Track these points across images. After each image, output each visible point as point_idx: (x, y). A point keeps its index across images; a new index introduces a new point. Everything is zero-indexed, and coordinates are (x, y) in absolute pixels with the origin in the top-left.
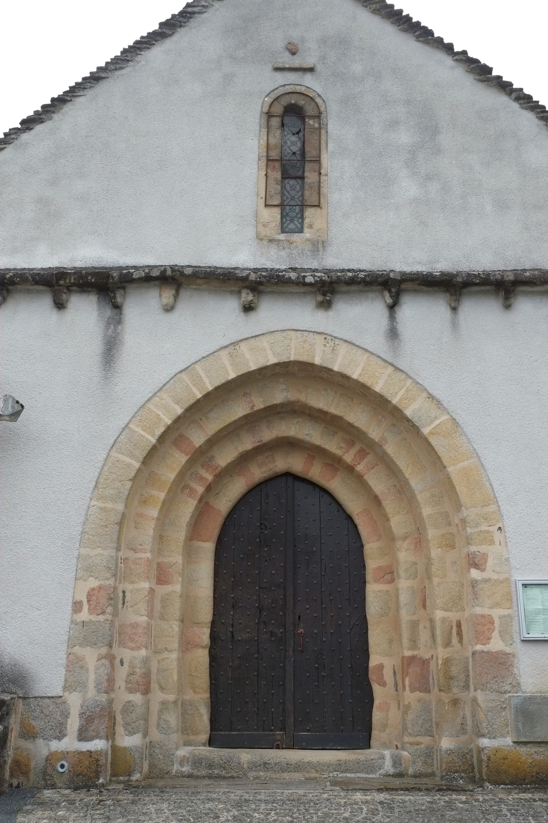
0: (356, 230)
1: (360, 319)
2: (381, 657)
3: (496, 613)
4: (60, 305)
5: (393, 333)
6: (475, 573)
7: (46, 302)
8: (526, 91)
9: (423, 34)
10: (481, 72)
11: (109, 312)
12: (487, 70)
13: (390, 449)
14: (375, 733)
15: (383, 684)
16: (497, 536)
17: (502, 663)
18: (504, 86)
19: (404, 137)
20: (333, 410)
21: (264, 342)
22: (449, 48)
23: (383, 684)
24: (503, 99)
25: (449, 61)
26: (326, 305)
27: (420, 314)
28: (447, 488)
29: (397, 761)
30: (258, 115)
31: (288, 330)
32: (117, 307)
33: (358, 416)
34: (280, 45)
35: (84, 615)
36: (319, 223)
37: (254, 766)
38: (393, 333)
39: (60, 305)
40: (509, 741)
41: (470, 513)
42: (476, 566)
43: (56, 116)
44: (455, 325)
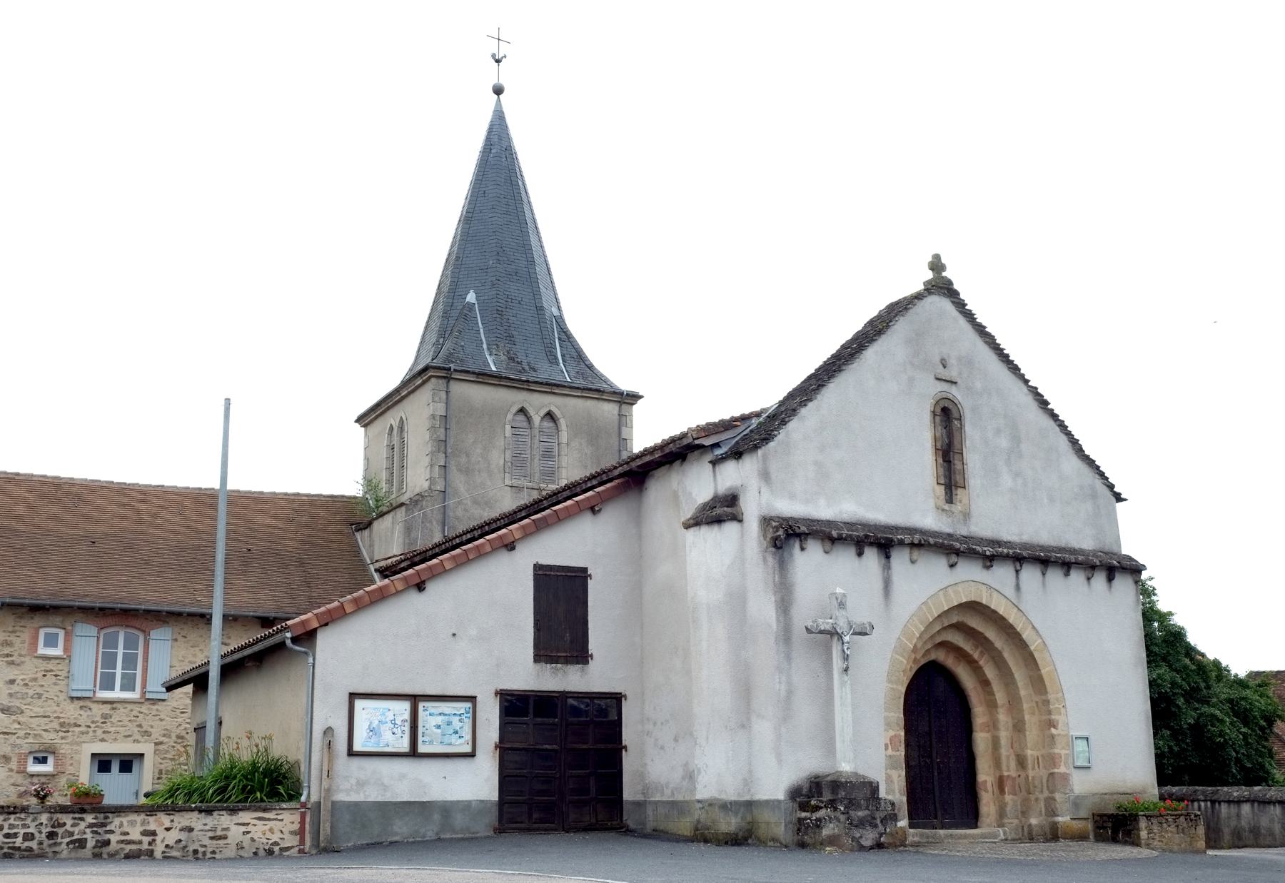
0: (992, 512)
1: (1002, 575)
2: (985, 775)
3: (1063, 752)
4: (860, 554)
5: (1018, 588)
6: (1053, 730)
7: (851, 552)
8: (956, 287)
9: (1014, 369)
10: (1043, 403)
11: (883, 561)
12: (1046, 403)
13: (1006, 655)
14: (981, 819)
15: (986, 791)
16: (1063, 711)
17: (1065, 777)
18: (1054, 416)
19: (1004, 443)
20: (980, 629)
21: (960, 588)
22: (1026, 382)
23: (986, 791)
24: (1052, 423)
25: (1025, 389)
26: (988, 568)
27: (1030, 575)
28: (1038, 683)
29: (1005, 833)
30: (927, 417)
31: (971, 581)
32: (888, 557)
33: (990, 633)
34: (937, 359)
35: (890, 752)
36: (965, 501)
37: (947, 836)
38: (1018, 588)
39: (860, 554)
40: (1067, 818)
41: (1051, 697)
42: (1054, 727)
43: (819, 397)
44: (1044, 584)
